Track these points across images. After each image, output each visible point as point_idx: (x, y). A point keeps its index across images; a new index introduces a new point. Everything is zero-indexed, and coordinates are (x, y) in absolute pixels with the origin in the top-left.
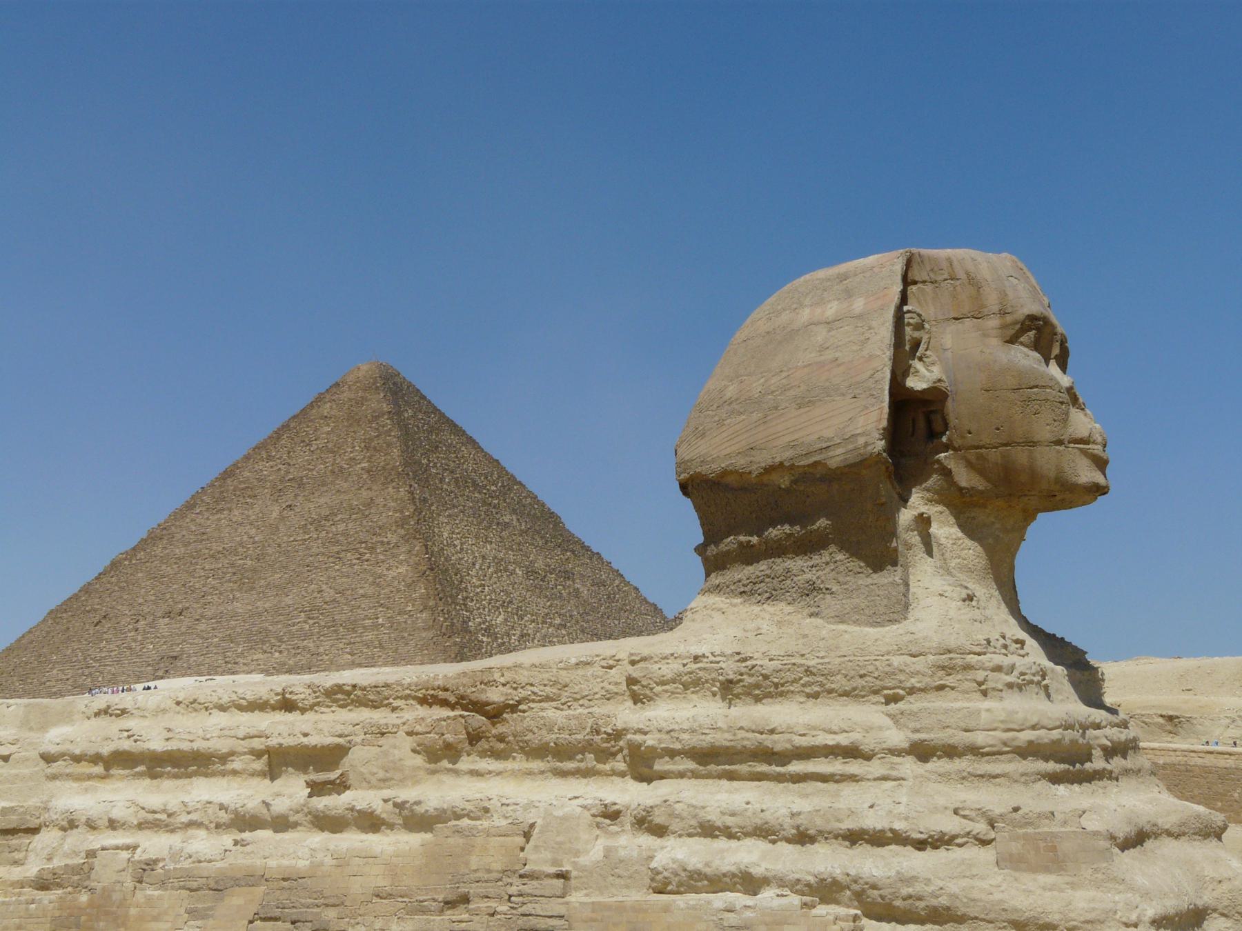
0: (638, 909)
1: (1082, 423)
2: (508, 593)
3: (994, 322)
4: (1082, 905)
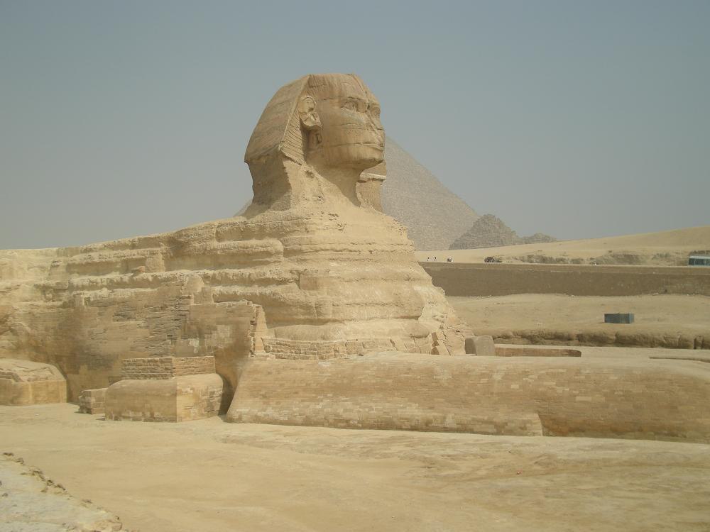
0: (208, 307)
3: (337, 100)
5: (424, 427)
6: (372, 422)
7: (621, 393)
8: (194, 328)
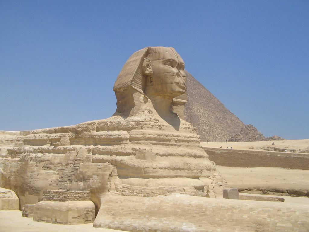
1: (178, 79)
2: (210, 122)
3: (161, 61)
4: (147, 165)
7: (301, 223)
8: (81, 176)
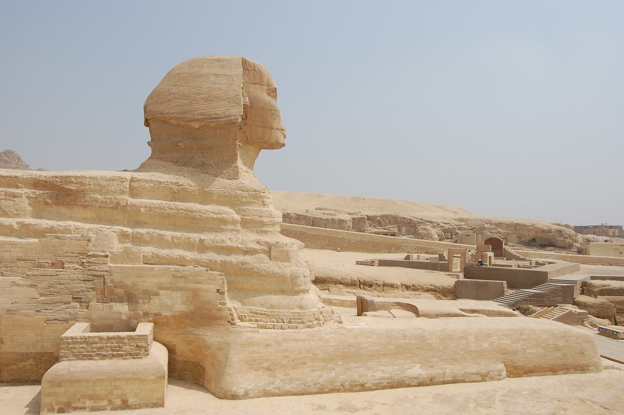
3: (266, 88)
5: (429, 382)
6: (385, 384)
